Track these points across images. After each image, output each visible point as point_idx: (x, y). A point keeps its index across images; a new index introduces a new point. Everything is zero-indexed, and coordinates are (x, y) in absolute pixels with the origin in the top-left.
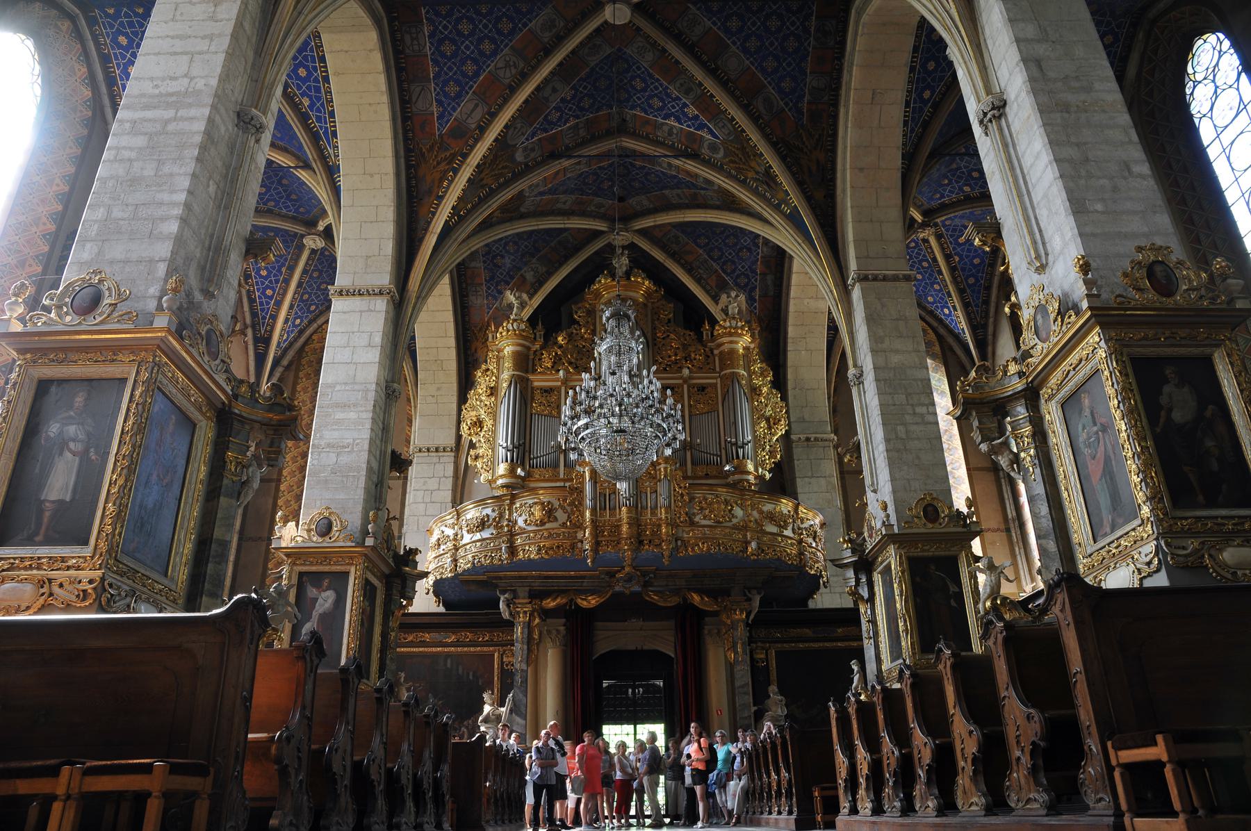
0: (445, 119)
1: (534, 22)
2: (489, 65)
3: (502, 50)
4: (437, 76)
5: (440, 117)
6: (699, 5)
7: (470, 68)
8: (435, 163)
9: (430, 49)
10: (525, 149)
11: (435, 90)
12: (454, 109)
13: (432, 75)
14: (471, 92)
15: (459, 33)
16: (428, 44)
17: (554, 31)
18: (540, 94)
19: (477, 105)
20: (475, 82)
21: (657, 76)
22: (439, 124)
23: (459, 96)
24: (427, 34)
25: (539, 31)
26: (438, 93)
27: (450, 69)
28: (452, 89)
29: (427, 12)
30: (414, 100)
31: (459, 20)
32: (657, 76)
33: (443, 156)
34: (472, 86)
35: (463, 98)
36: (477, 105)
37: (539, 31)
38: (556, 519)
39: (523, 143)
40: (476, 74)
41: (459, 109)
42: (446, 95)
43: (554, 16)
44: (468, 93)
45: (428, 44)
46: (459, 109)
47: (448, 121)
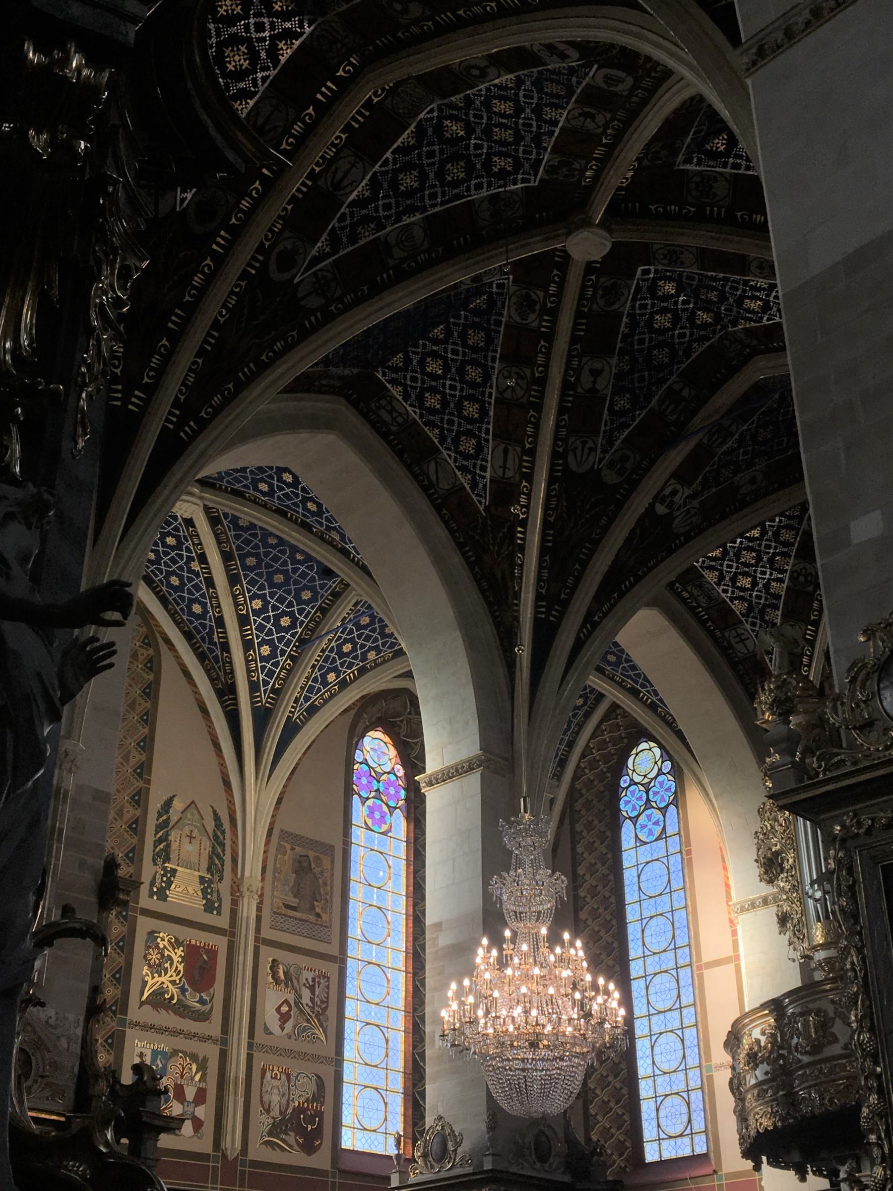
0: (481, 486)
1: (505, 313)
2: (490, 394)
3: (493, 368)
4: (442, 440)
5: (474, 485)
6: (695, 160)
7: (471, 409)
8: (496, 548)
9: (415, 412)
10: (611, 465)
11: (450, 456)
12: (483, 469)
13: (436, 441)
14: (490, 437)
15: (433, 376)
16: (409, 409)
17: (537, 307)
18: (579, 390)
19: (506, 451)
20: (488, 423)
21: (721, 275)
22: (477, 495)
23: (479, 449)
24: (400, 398)
25: (518, 319)
26: (456, 458)
27: (451, 423)
28: (468, 445)
29: (384, 375)
30: (434, 478)
31: (422, 363)
32: (721, 275)
33: (501, 535)
34: (487, 430)
35: (486, 450)
36: (506, 451)
37: (518, 319)
38: (836, 1040)
39: (601, 460)
40: (483, 412)
41: (489, 465)
42: (466, 456)
43: (524, 292)
44: (487, 440)
45: (409, 409)
46: (489, 465)
47: (485, 486)
